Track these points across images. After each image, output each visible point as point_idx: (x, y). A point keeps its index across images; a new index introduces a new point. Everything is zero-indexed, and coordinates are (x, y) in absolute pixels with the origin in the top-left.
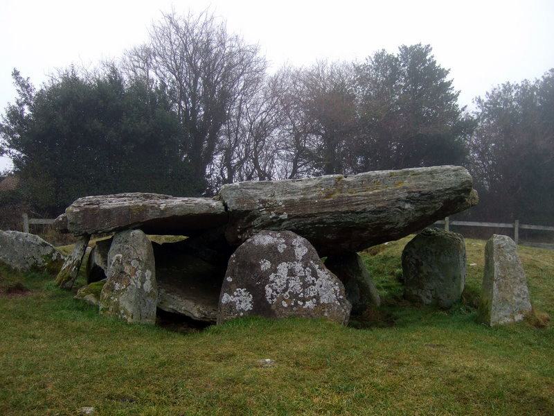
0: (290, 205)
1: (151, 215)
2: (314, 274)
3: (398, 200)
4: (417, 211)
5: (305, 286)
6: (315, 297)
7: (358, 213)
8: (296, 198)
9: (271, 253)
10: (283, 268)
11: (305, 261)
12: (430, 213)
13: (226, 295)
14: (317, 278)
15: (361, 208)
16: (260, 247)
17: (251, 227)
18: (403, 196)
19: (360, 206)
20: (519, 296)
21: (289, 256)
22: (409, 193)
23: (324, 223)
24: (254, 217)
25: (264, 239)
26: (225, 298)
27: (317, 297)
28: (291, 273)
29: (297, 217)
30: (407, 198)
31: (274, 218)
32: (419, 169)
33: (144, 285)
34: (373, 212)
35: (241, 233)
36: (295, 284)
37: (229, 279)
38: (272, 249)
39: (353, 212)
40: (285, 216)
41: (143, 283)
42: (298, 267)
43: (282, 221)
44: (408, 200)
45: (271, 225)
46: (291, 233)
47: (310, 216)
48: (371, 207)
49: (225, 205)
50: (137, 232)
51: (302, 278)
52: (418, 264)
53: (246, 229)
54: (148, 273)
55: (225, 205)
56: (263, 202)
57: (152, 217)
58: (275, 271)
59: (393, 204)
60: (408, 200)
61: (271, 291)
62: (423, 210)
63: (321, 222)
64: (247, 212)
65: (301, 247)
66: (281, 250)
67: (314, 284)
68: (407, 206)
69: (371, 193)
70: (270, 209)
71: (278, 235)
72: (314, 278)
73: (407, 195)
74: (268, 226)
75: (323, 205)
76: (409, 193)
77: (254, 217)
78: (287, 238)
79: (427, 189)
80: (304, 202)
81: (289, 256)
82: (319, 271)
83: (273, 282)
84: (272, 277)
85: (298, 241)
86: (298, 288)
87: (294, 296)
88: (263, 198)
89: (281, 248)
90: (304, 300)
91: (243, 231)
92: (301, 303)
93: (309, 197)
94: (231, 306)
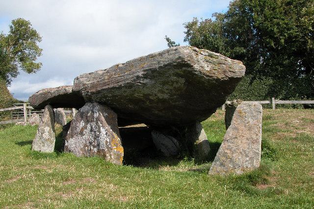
0: (93, 86)
3: (138, 77)
15: (119, 84)
18: (140, 74)
22: (144, 71)
30: (143, 75)
31: (87, 95)
37: (68, 132)
42: (94, 124)
44: (145, 77)
56: (84, 85)
59: (135, 80)
68: (146, 81)
70: (86, 88)
73: (143, 73)
75: (105, 84)
76: (144, 71)
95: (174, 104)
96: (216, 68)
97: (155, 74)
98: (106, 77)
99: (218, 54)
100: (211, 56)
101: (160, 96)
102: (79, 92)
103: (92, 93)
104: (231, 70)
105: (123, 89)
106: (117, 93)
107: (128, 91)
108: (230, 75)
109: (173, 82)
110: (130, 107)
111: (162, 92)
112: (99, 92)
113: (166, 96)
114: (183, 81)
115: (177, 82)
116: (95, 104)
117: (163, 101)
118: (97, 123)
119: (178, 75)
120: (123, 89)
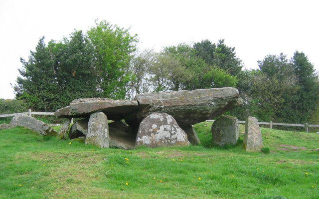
0: (165, 102)
2: (175, 130)
3: (209, 100)
4: (217, 106)
5: (172, 134)
6: (175, 139)
7: (193, 106)
8: (168, 99)
10: (162, 127)
11: (172, 124)
12: (222, 106)
13: (139, 138)
16: (153, 119)
17: (149, 111)
21: (165, 122)
24: (150, 107)
25: (154, 116)
26: (139, 139)
27: (176, 139)
28: (165, 130)
29: (168, 107)
34: (199, 105)
35: (144, 114)
37: (140, 132)
39: (191, 105)
40: (163, 107)
43: (162, 108)
45: (159, 110)
46: (165, 113)
47: (173, 106)
48: (198, 103)
49: (138, 102)
50: (101, 113)
51: (170, 132)
52: (219, 131)
53: (146, 112)
54: (106, 130)
55: (138, 102)
56: (154, 101)
62: (220, 105)
63: (178, 109)
64: (148, 105)
65: (170, 119)
66: (161, 120)
68: (213, 103)
70: (157, 103)
71: (160, 114)
74: (155, 111)
77: (150, 107)
78: (164, 116)
80: (171, 101)
81: (165, 122)
88: (154, 99)
89: (162, 119)
91: (145, 113)
93: (173, 99)
94: (141, 143)
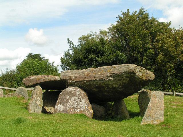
0: (76, 78)
1: (41, 81)
3: (107, 76)
5: (78, 104)
9: (71, 94)
10: (73, 98)
14: (81, 102)
15: (95, 79)
18: (109, 75)
19: (95, 78)
20: (158, 114)
21: (74, 95)
22: (111, 73)
23: (86, 84)
26: (56, 107)
28: (75, 100)
31: (71, 82)
32: (117, 66)
33: (37, 102)
36: (75, 104)
37: (58, 101)
38: (71, 92)
41: (36, 101)
42: (77, 98)
43: (74, 83)
44: (111, 76)
45: (72, 85)
48: (98, 79)
56: (69, 77)
57: (41, 81)
58: (71, 99)
59: (105, 77)
60: (111, 76)
61: (68, 105)
66: (73, 92)
67: (80, 104)
68: (111, 78)
69: (99, 74)
70: (70, 79)
71: (73, 88)
72: (80, 102)
75: (85, 78)
76: (111, 73)
79: (117, 72)
82: (82, 100)
83: (69, 103)
84: (69, 101)
85: (78, 89)
86: (76, 106)
87: (74, 107)
88: (70, 76)
90: (77, 109)
92: (76, 110)
95: (118, 90)
96: (144, 75)
97: (116, 76)
98: (86, 75)
99: (144, 69)
100: (142, 69)
101: (115, 86)
102: (65, 80)
103: (76, 82)
104: (149, 76)
105: (97, 81)
106: (93, 83)
107: (100, 82)
108: (149, 78)
109: (124, 80)
110: (94, 90)
111: (116, 84)
112: (81, 81)
113: (117, 86)
114: (128, 79)
115: (125, 80)
116: (77, 87)
117: (115, 88)
118: (79, 97)
119: (127, 77)
120: (97, 81)
